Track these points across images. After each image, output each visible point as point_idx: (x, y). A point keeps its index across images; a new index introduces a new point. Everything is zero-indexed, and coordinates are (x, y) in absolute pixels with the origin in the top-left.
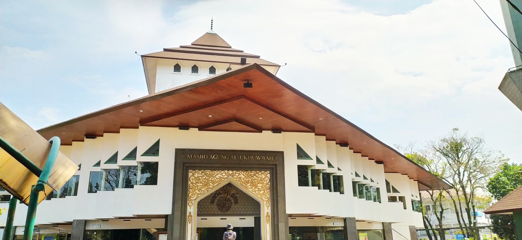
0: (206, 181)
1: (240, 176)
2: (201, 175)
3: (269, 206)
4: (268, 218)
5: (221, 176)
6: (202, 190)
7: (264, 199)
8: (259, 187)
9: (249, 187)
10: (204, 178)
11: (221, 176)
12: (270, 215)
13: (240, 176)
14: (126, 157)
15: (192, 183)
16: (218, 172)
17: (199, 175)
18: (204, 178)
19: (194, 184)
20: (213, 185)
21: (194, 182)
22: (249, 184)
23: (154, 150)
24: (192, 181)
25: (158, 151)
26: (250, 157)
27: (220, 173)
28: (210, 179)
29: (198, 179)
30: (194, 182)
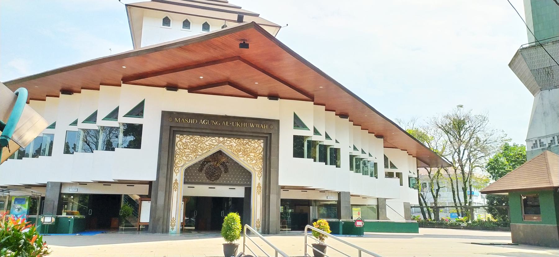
0: (195, 147)
1: (231, 144)
2: (189, 141)
3: (261, 176)
4: (259, 189)
5: (211, 142)
6: (189, 156)
7: (256, 169)
8: (251, 157)
9: (241, 156)
10: (192, 143)
11: (211, 142)
12: (261, 185)
13: (231, 144)
14: (106, 117)
15: (179, 149)
16: (208, 138)
17: (187, 141)
18: (192, 143)
19: (181, 150)
20: (202, 152)
21: (182, 148)
22: (241, 153)
23: (138, 111)
24: (179, 146)
25: (142, 112)
26: (243, 124)
27: (210, 140)
28: (199, 145)
29: (186, 144)
30: (182, 148)
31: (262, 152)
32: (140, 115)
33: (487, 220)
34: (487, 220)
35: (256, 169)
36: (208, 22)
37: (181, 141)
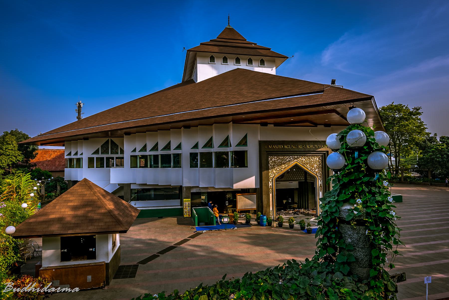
0: (280, 163)
1: (302, 159)
2: (276, 159)
3: (321, 180)
4: (321, 188)
5: (289, 159)
6: (277, 170)
7: (318, 175)
8: (315, 167)
9: (309, 167)
10: (278, 161)
11: (289, 159)
12: (322, 186)
13: (302, 159)
14: (193, 147)
15: (271, 165)
16: (288, 157)
17: (275, 159)
18: (278, 161)
19: (272, 166)
20: (284, 166)
21: (272, 164)
22: (308, 165)
23: (244, 142)
24: (270, 164)
25: (246, 142)
26: (311, 146)
27: (289, 158)
28: (283, 162)
29: (274, 162)
30: (272, 164)
31: (321, 163)
32: (245, 144)
33: (358, 279)
34: (358, 279)
35: (318, 175)
36: (226, 56)
37: (273, 159)
